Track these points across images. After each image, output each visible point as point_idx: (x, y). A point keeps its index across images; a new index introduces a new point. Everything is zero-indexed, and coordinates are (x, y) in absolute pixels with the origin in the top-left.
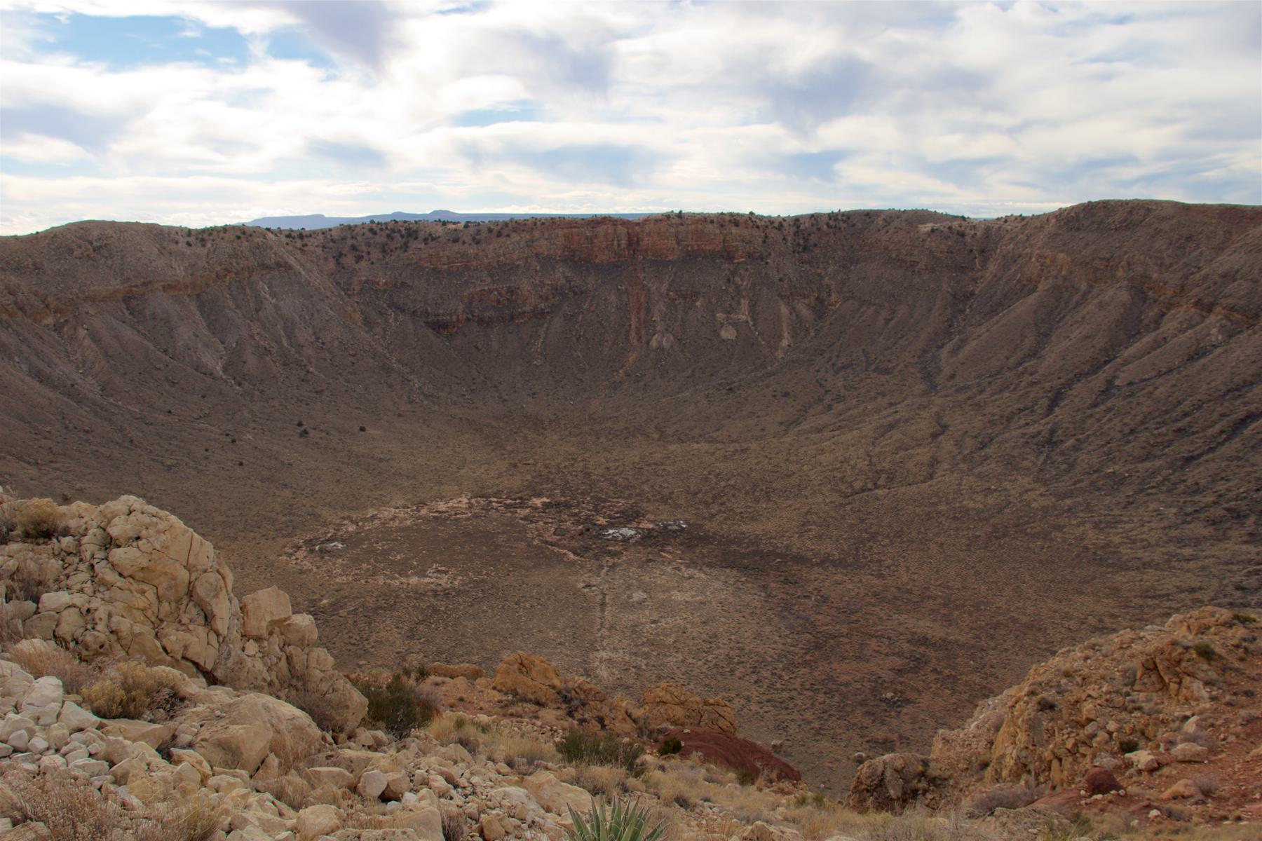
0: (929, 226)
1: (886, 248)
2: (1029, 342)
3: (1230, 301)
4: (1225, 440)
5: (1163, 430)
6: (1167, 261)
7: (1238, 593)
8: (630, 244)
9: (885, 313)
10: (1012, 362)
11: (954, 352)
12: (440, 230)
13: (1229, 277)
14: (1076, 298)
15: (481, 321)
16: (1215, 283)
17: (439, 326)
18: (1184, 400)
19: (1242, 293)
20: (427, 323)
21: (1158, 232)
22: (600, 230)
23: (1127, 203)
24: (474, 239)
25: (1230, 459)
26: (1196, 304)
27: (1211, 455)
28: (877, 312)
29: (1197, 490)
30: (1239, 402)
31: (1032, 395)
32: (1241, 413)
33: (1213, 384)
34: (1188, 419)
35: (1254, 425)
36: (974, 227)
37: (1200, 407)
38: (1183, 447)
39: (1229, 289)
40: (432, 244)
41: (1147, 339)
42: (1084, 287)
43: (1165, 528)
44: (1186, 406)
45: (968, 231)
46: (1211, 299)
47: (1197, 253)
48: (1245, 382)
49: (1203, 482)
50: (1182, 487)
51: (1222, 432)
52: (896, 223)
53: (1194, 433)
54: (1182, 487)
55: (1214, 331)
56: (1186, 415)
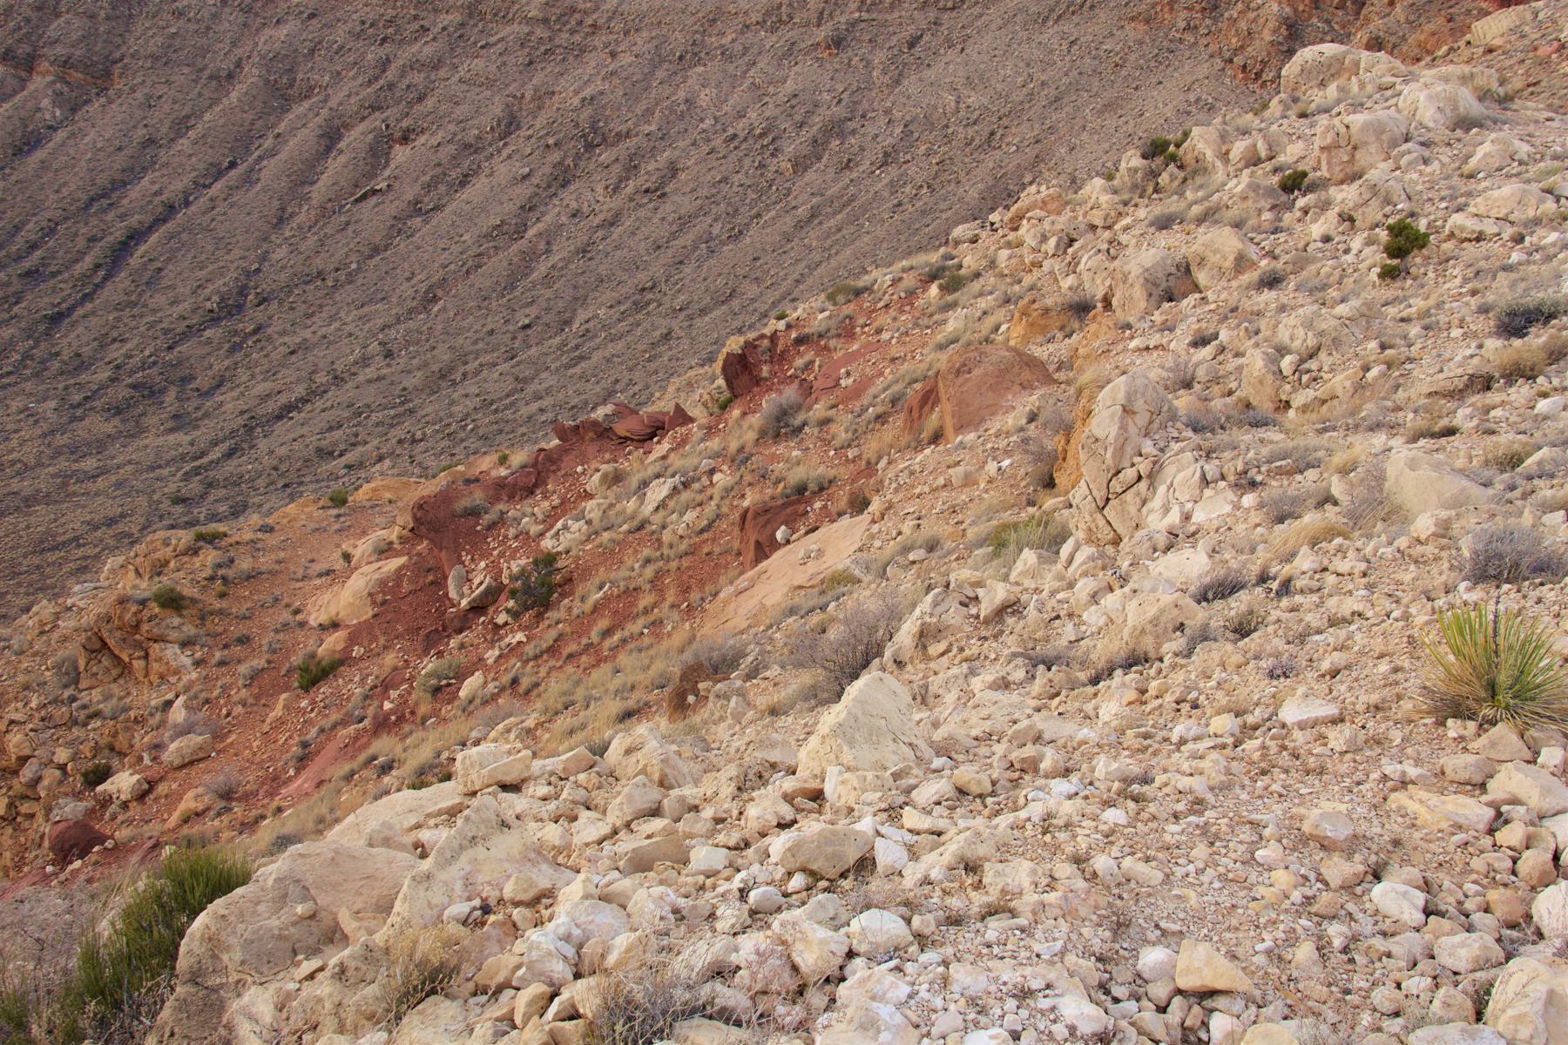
3: (59, 50)
4: (105, 279)
7: (179, 509)
16: (28, 20)
18: (24, 223)
25: (119, 307)
27: (89, 306)
29: (81, 364)
30: (110, 216)
32: (118, 233)
33: (65, 192)
34: (38, 253)
35: (143, 248)
38: (42, 300)
39: (54, 29)
43: (44, 435)
44: (30, 231)
46: (28, 49)
48: (113, 182)
49: (86, 351)
50: (56, 365)
51: (98, 266)
53: (54, 275)
54: (56, 365)
55: (45, 103)
56: (34, 246)
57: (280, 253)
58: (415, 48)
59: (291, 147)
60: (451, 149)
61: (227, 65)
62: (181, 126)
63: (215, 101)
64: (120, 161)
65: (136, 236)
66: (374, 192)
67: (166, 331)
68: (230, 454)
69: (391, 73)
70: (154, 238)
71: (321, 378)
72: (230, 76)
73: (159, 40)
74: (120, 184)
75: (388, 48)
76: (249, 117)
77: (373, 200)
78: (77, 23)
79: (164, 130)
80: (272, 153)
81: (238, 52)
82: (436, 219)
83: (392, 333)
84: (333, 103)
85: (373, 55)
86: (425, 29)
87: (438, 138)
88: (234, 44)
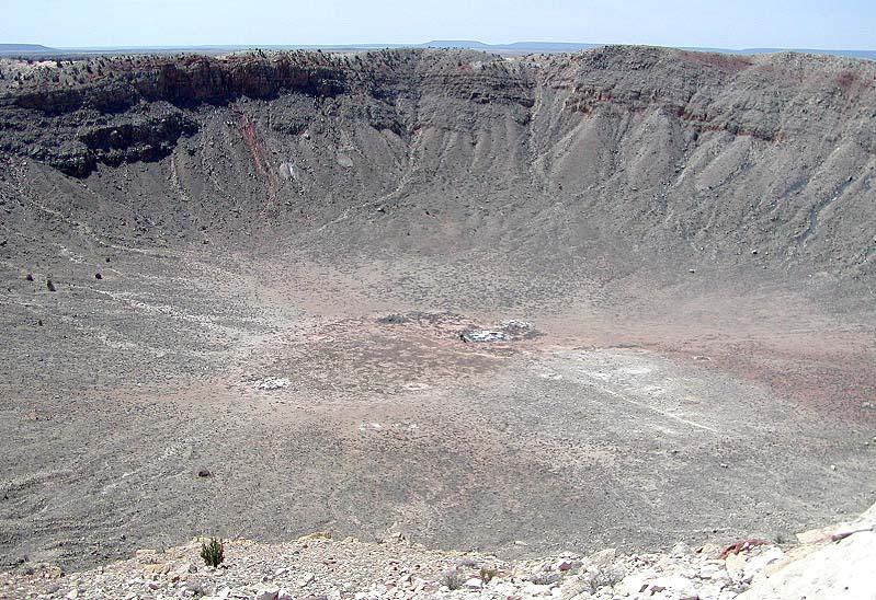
0: (477, 66)
2: (606, 157)
8: (223, 82)
9: (467, 139)
10: (602, 174)
11: (547, 168)
12: (27, 69)
14: (624, 122)
15: (108, 162)
17: (70, 171)
19: (758, 119)
20: (54, 166)
22: (194, 66)
23: (638, 48)
24: (75, 78)
26: (726, 128)
30: (800, 197)
32: (808, 205)
35: (825, 213)
39: (746, 115)
40: (31, 83)
41: (700, 154)
42: (625, 117)
45: (507, 67)
47: (706, 87)
61: (833, 136)
62: (819, 160)
64: (795, 175)
72: (835, 140)
74: (798, 185)
78: (757, 113)
81: (839, 130)
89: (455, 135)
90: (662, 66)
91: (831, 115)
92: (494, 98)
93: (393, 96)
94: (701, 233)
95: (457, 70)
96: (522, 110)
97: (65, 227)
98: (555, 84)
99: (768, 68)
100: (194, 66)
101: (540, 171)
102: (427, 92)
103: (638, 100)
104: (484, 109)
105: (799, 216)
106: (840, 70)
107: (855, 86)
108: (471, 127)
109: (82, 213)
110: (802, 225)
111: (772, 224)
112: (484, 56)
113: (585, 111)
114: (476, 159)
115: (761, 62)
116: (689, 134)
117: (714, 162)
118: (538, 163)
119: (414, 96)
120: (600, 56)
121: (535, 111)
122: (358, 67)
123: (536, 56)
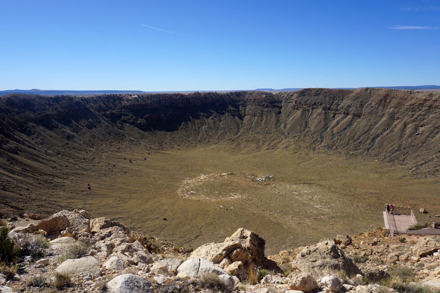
1: (254, 101)
2: (304, 124)
5: (355, 143)
6: (331, 103)
8: (187, 102)
10: (302, 129)
11: (285, 127)
13: (349, 106)
14: (310, 113)
21: (325, 97)
22: (178, 97)
28: (258, 118)
31: (315, 137)
32: (372, 137)
35: (377, 140)
36: (275, 95)
37: (360, 137)
39: (351, 109)
41: (335, 122)
52: (254, 95)
53: (364, 143)
56: (358, 139)
57: (404, 142)
58: (420, 112)
59: (399, 126)
60: (433, 128)
61: (381, 115)
62: (376, 123)
63: (380, 120)
64: (367, 127)
65: (374, 139)
66: (419, 134)
67: (390, 152)
68: (417, 169)
69: (415, 116)
70: (379, 138)
71: (426, 160)
73: (369, 111)
74: (369, 130)
75: (413, 113)
76: (389, 122)
77: (420, 135)
78: (355, 108)
79: (373, 123)
80: (395, 127)
82: (434, 139)
83: (437, 155)
84: (404, 120)
85: (410, 113)
86: (420, 110)
87: (430, 126)
88: (382, 111)
89: (256, 118)
90: (323, 94)
91: (381, 108)
92: (269, 106)
93: (238, 106)
94: (334, 147)
95: (258, 98)
96: (278, 110)
97: (137, 144)
98: (288, 101)
99: (359, 94)
100: (178, 97)
101: (283, 128)
102: (249, 105)
103: (314, 106)
104: (266, 109)
105: (368, 142)
106: (385, 93)
107: (389, 98)
108: (262, 115)
109: (143, 140)
110: (370, 144)
111: (359, 144)
112: (266, 94)
113: (297, 109)
114: (263, 125)
115: (355, 92)
116: (331, 116)
117: (339, 125)
118: (282, 126)
119: (245, 106)
120: (303, 92)
121: (282, 110)
122: (228, 97)
123: (283, 93)
